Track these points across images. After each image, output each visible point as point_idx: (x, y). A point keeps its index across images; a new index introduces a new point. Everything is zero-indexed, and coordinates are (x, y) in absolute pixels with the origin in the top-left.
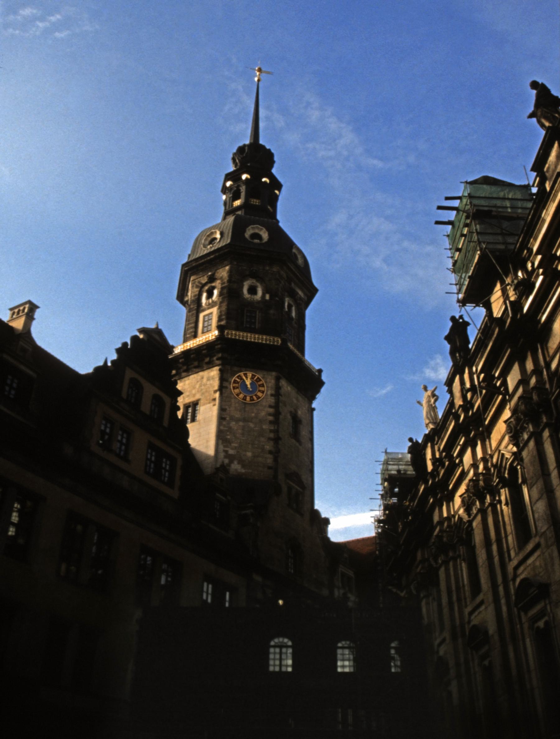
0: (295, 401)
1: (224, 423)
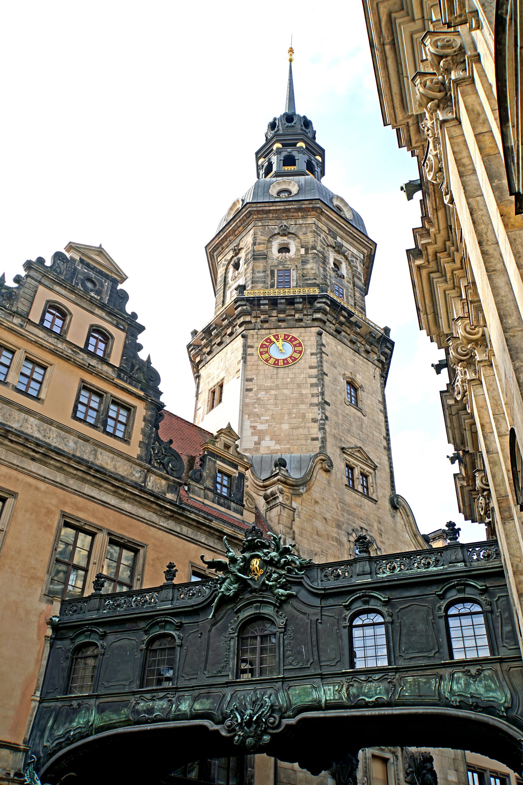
1: (250, 394)
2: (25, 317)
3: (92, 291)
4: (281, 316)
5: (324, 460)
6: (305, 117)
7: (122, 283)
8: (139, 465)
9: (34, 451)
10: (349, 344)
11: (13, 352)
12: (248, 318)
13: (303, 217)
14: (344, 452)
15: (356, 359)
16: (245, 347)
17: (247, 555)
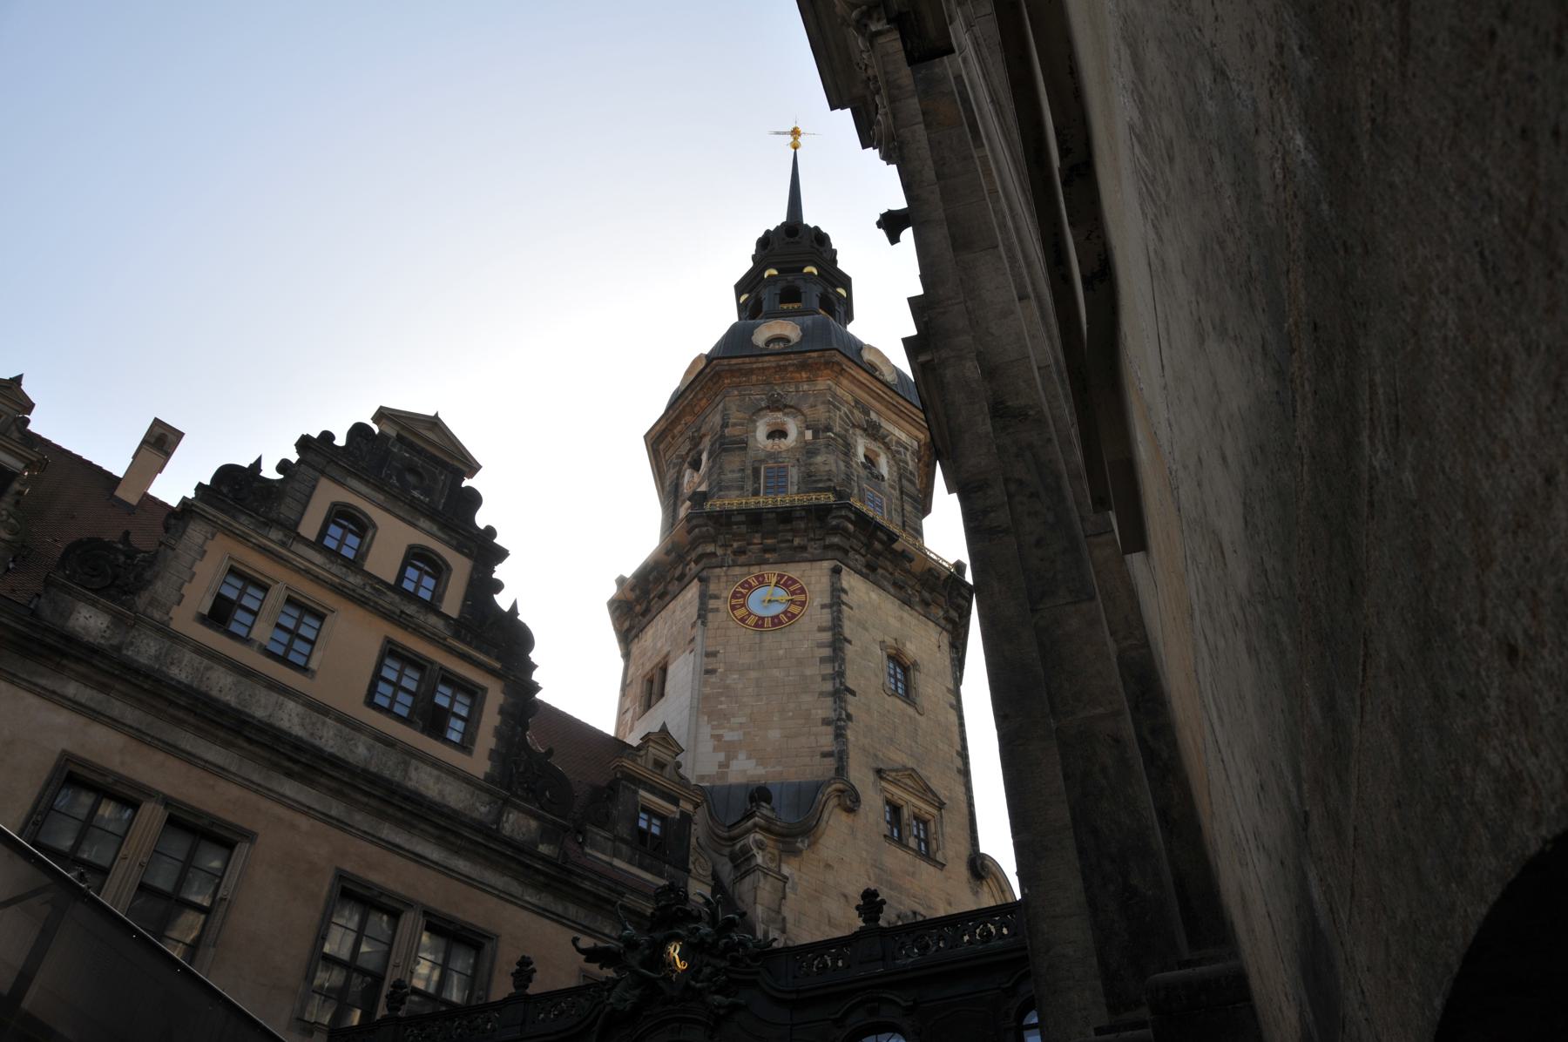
0: (896, 624)
1: (713, 679)
2: (291, 529)
3: (415, 488)
4: (769, 541)
5: (842, 791)
6: (816, 228)
7: (471, 476)
8: (488, 791)
9: (290, 759)
10: (892, 590)
11: (265, 588)
12: (710, 548)
13: (809, 380)
14: (881, 778)
15: (905, 615)
16: (704, 597)
17: (658, 935)
